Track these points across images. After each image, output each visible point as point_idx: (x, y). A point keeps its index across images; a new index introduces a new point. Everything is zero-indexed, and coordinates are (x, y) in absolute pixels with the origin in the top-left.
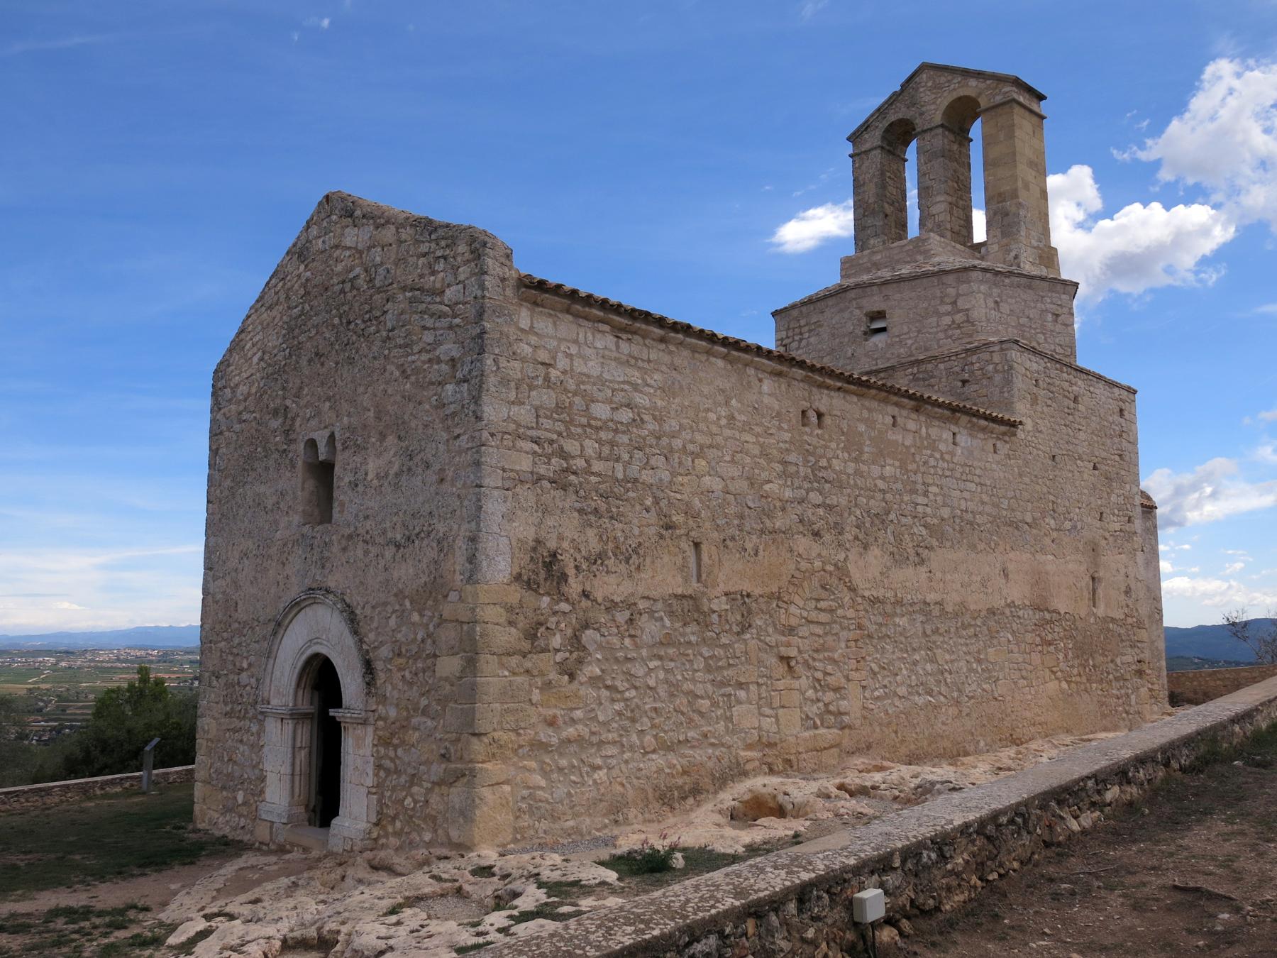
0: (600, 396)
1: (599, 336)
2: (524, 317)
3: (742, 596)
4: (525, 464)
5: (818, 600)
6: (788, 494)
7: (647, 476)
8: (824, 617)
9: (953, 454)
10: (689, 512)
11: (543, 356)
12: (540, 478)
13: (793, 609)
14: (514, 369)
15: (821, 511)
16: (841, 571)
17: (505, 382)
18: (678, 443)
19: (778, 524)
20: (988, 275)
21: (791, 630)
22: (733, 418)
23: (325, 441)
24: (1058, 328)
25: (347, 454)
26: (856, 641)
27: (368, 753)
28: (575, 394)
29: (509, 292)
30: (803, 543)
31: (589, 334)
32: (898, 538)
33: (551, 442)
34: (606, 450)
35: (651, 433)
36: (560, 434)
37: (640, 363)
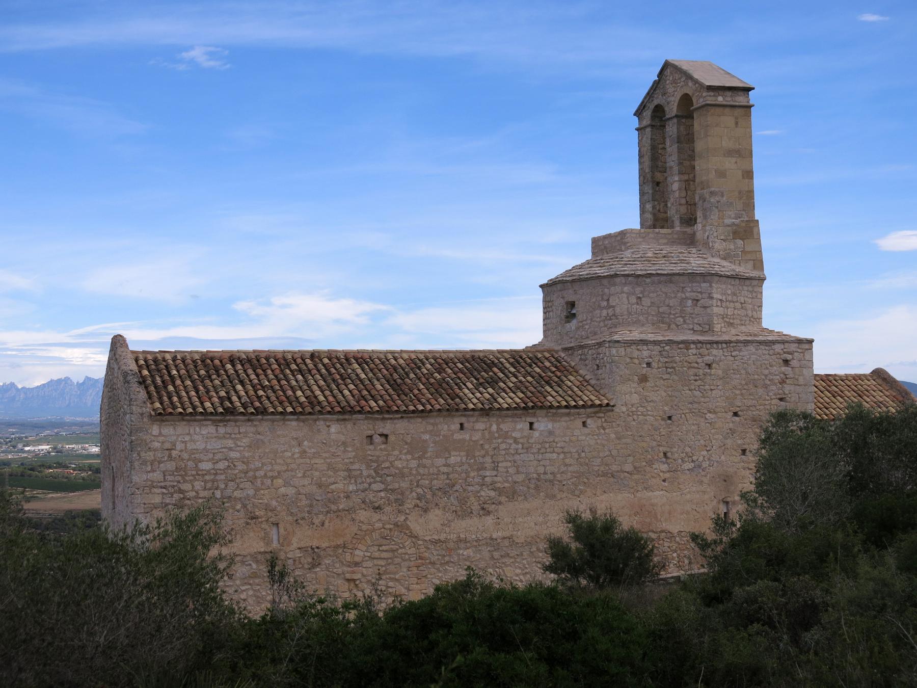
0: (205, 458)
1: (203, 428)
2: (155, 430)
3: (313, 549)
4: (157, 500)
5: (381, 546)
6: (352, 488)
7: (237, 494)
8: (384, 555)
9: (529, 437)
10: (268, 508)
11: (168, 445)
12: (167, 505)
13: (357, 552)
14: (150, 456)
15: (382, 494)
16: (401, 527)
17: (144, 463)
18: (258, 474)
19: (341, 507)
20: (630, 278)
21: (356, 564)
22: (305, 452)
24: (698, 310)
26: (418, 567)
28: (188, 460)
29: (145, 420)
30: (363, 515)
31: (197, 429)
32: (463, 501)
33: (173, 486)
34: (209, 485)
35: (241, 471)
36: (179, 482)
37: (233, 436)
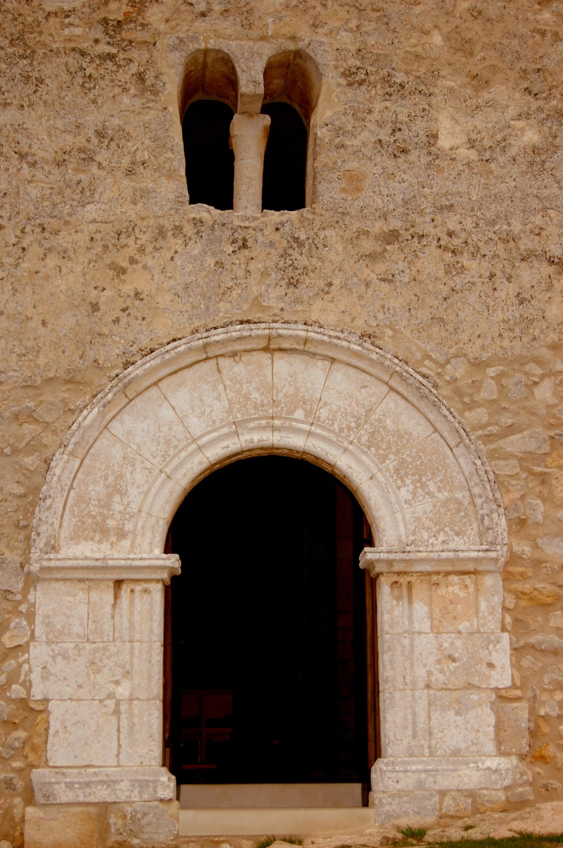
23: (260, 66)
25: (361, 94)
27: (493, 625)
